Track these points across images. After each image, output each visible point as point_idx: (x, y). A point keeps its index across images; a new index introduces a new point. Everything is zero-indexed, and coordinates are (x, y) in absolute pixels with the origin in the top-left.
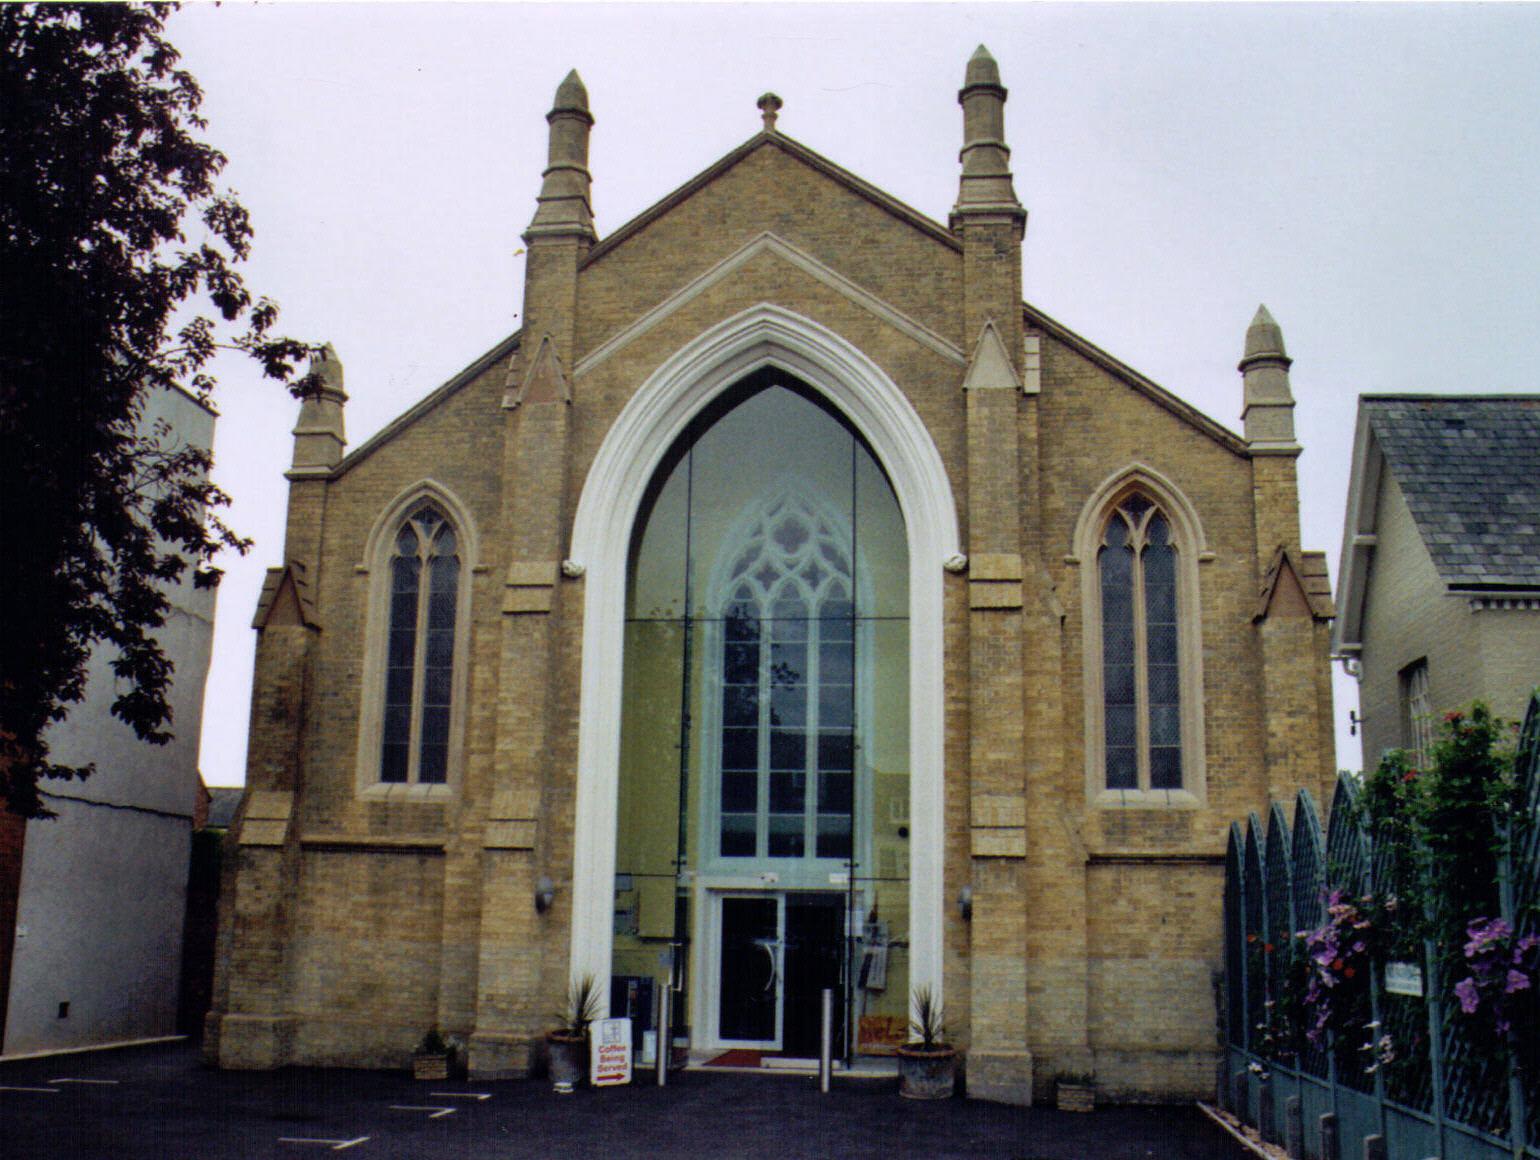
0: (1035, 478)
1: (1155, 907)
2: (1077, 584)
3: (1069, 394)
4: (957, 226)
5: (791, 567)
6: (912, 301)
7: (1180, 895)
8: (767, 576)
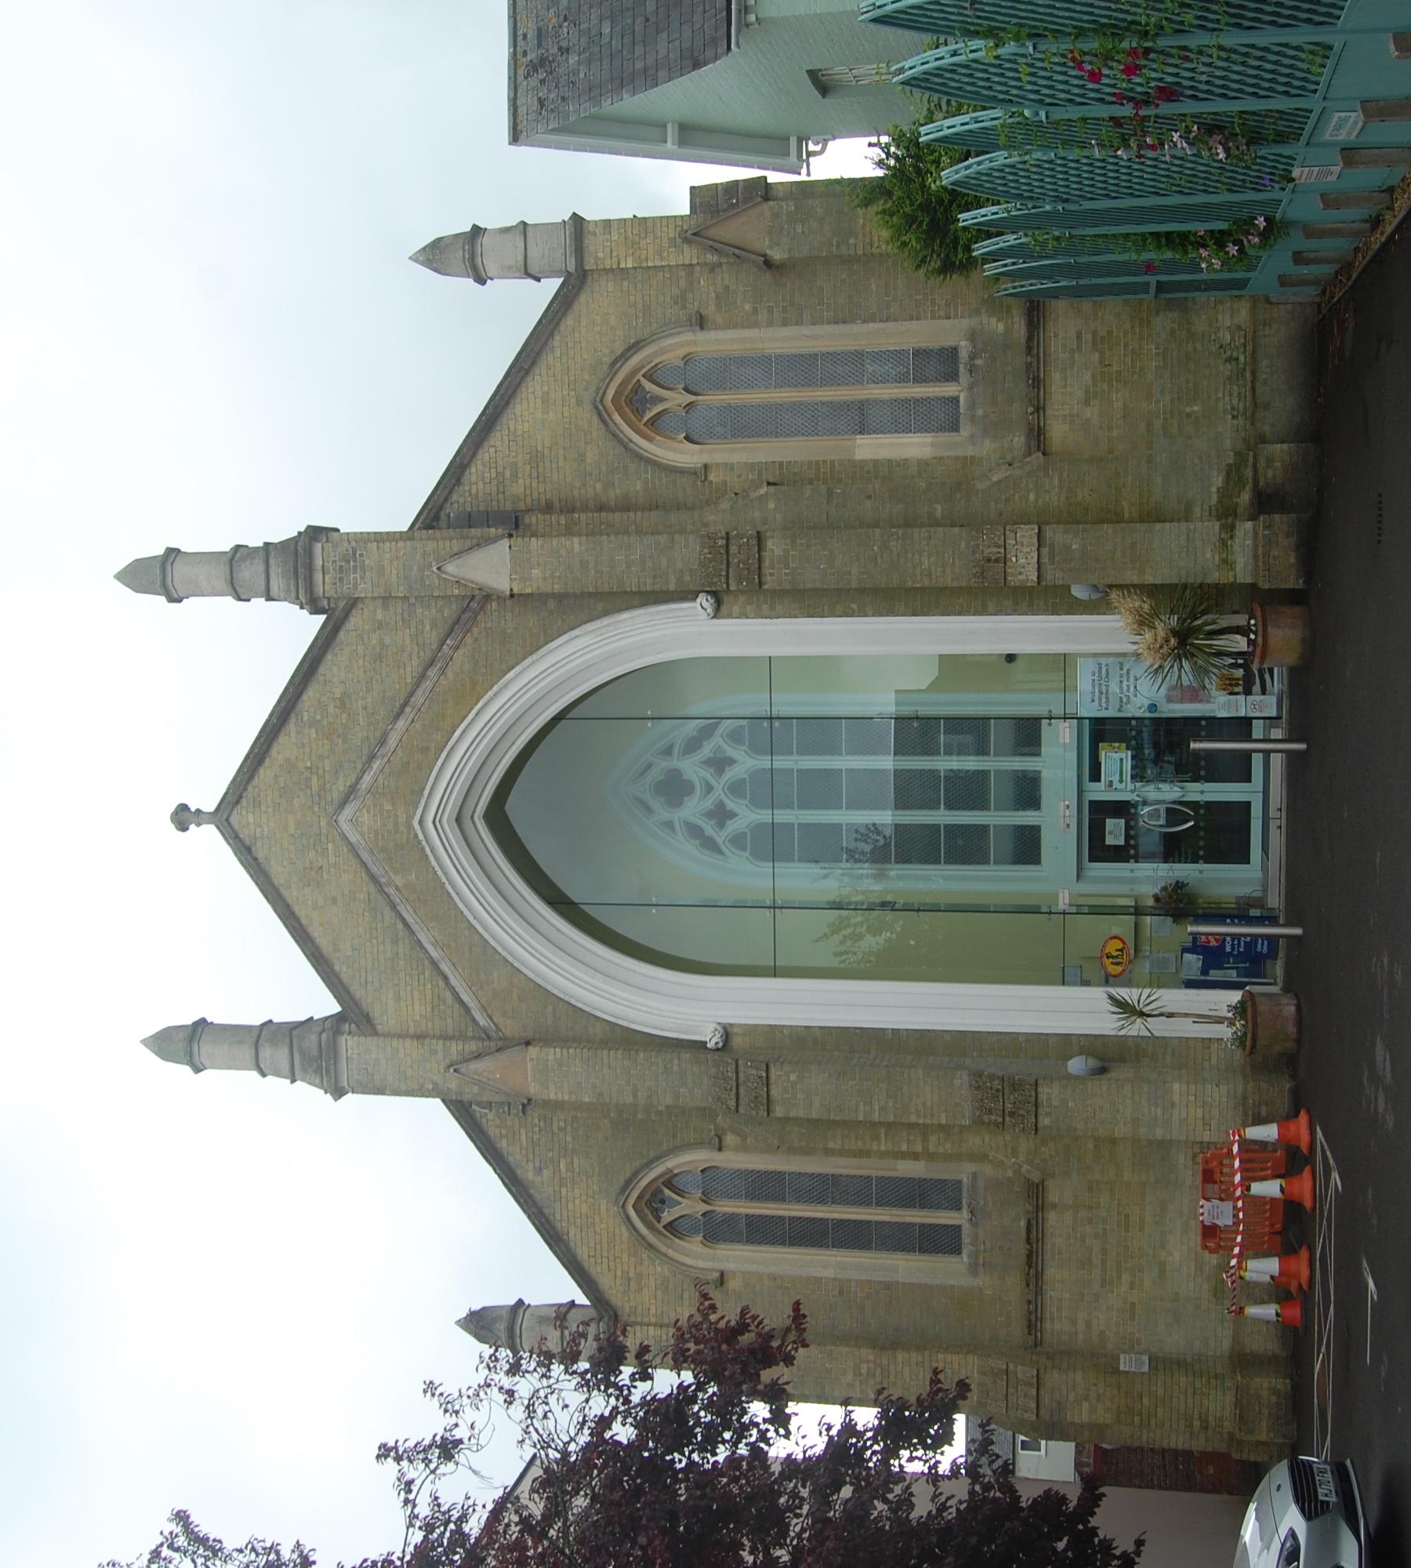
0: (610, 516)
1: (1093, 375)
2: (729, 467)
3: (515, 477)
4: (325, 603)
5: (709, 789)
6: (411, 654)
7: (1079, 348)
8: (721, 814)
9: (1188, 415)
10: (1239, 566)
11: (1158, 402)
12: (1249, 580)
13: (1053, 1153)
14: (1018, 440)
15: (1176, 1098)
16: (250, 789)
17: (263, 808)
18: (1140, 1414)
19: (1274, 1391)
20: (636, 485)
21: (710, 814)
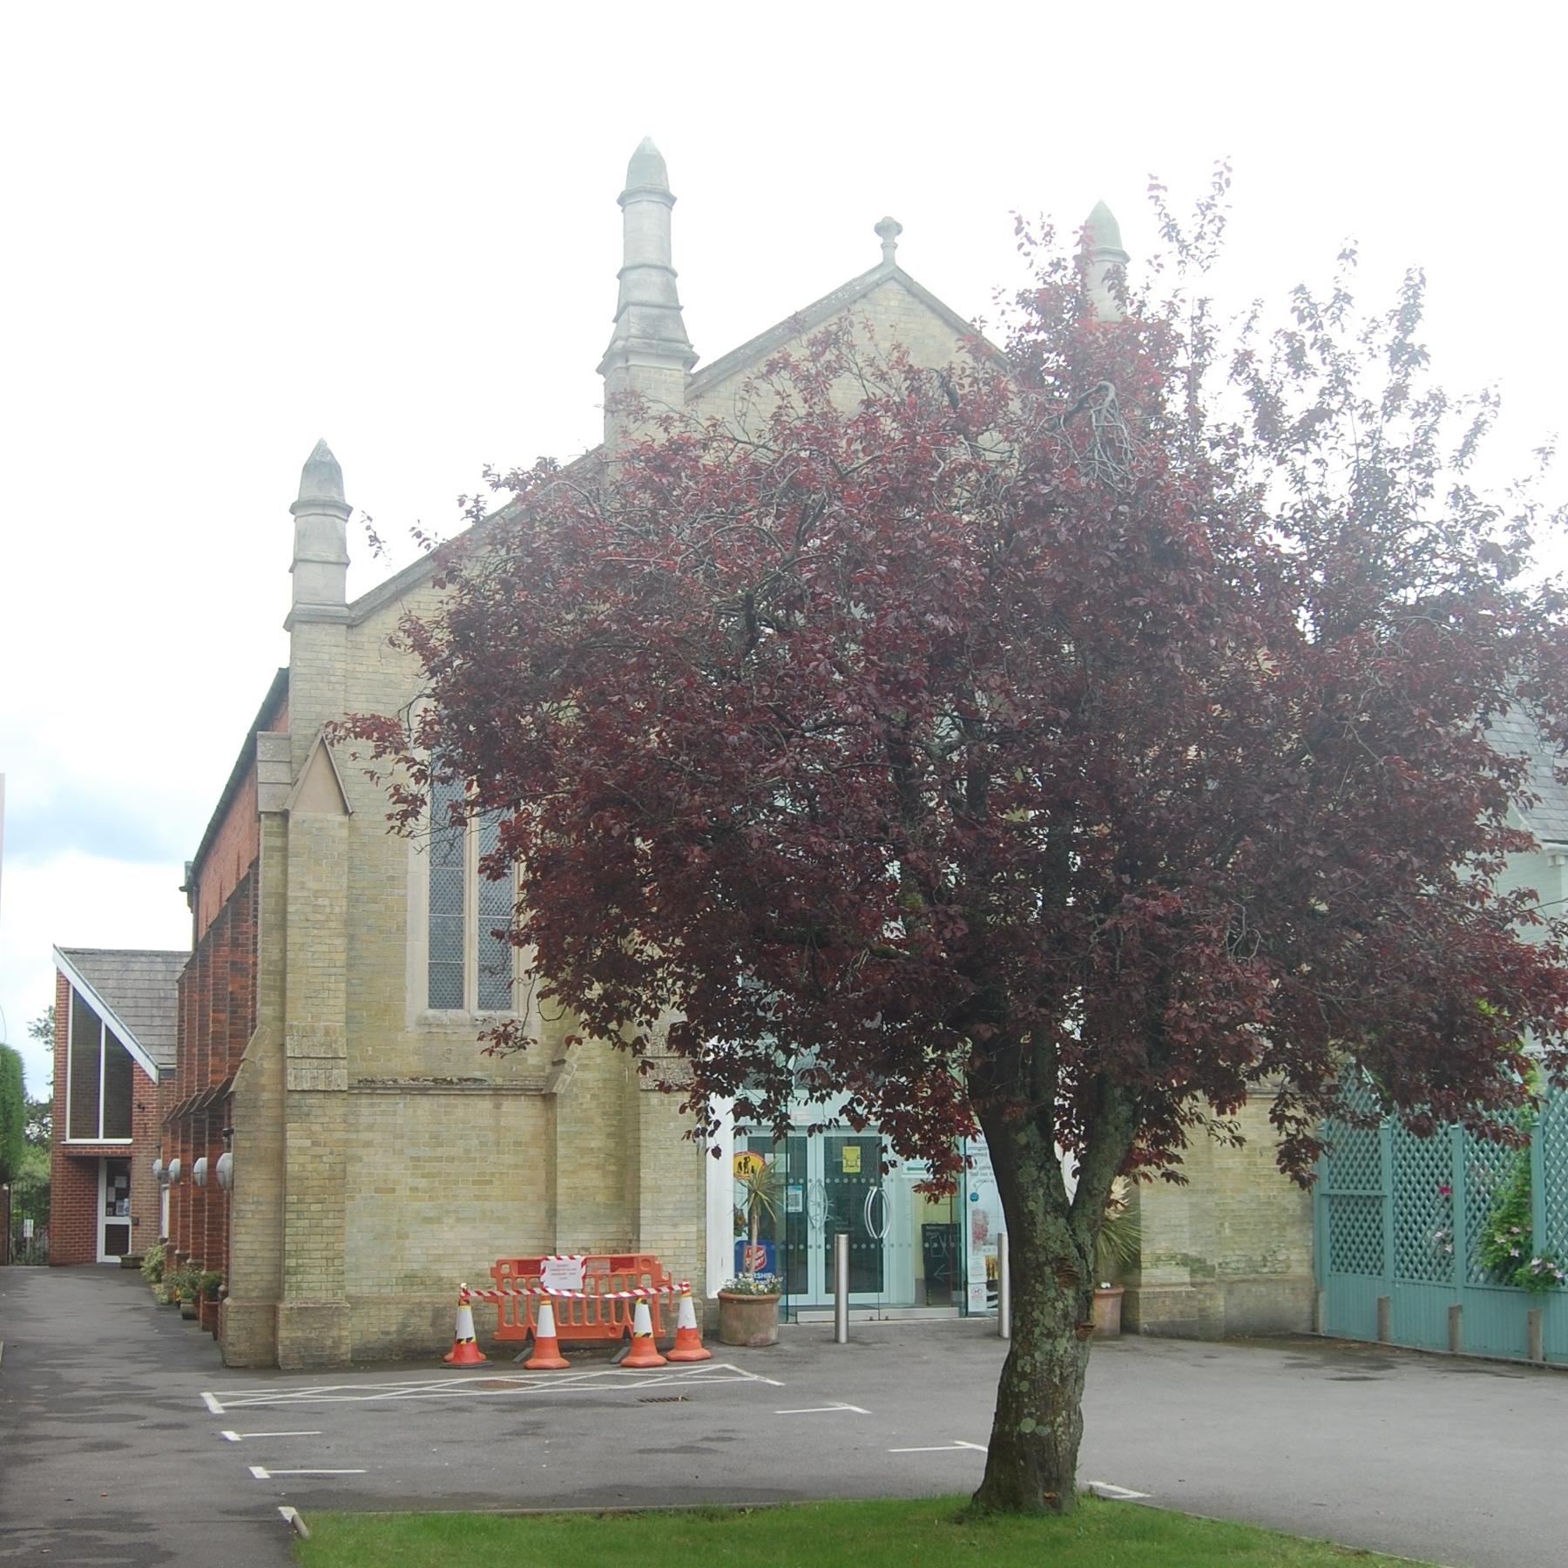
9: (1222, 1225)
10: (1154, 1271)
11: (1233, 1198)
12: (1144, 1280)
13: (584, 1106)
15: (682, 1228)
16: (922, 307)
17: (904, 318)
18: (300, 1202)
19: (337, 1343)
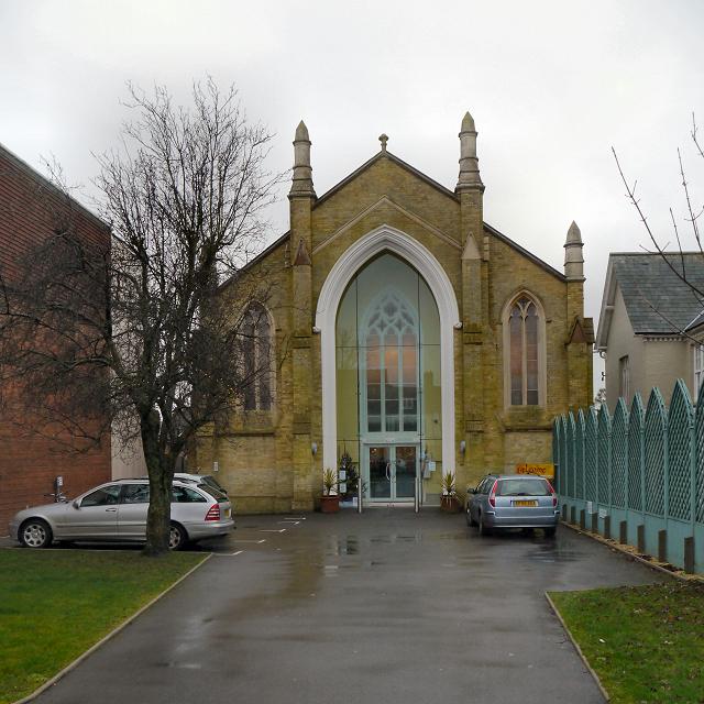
2: (502, 331)
5: (391, 321)
14: (508, 424)
20: (497, 298)
21: (382, 322)
